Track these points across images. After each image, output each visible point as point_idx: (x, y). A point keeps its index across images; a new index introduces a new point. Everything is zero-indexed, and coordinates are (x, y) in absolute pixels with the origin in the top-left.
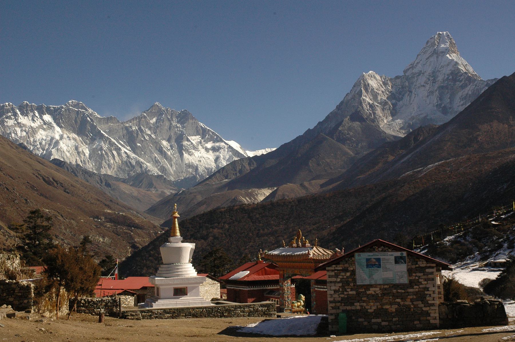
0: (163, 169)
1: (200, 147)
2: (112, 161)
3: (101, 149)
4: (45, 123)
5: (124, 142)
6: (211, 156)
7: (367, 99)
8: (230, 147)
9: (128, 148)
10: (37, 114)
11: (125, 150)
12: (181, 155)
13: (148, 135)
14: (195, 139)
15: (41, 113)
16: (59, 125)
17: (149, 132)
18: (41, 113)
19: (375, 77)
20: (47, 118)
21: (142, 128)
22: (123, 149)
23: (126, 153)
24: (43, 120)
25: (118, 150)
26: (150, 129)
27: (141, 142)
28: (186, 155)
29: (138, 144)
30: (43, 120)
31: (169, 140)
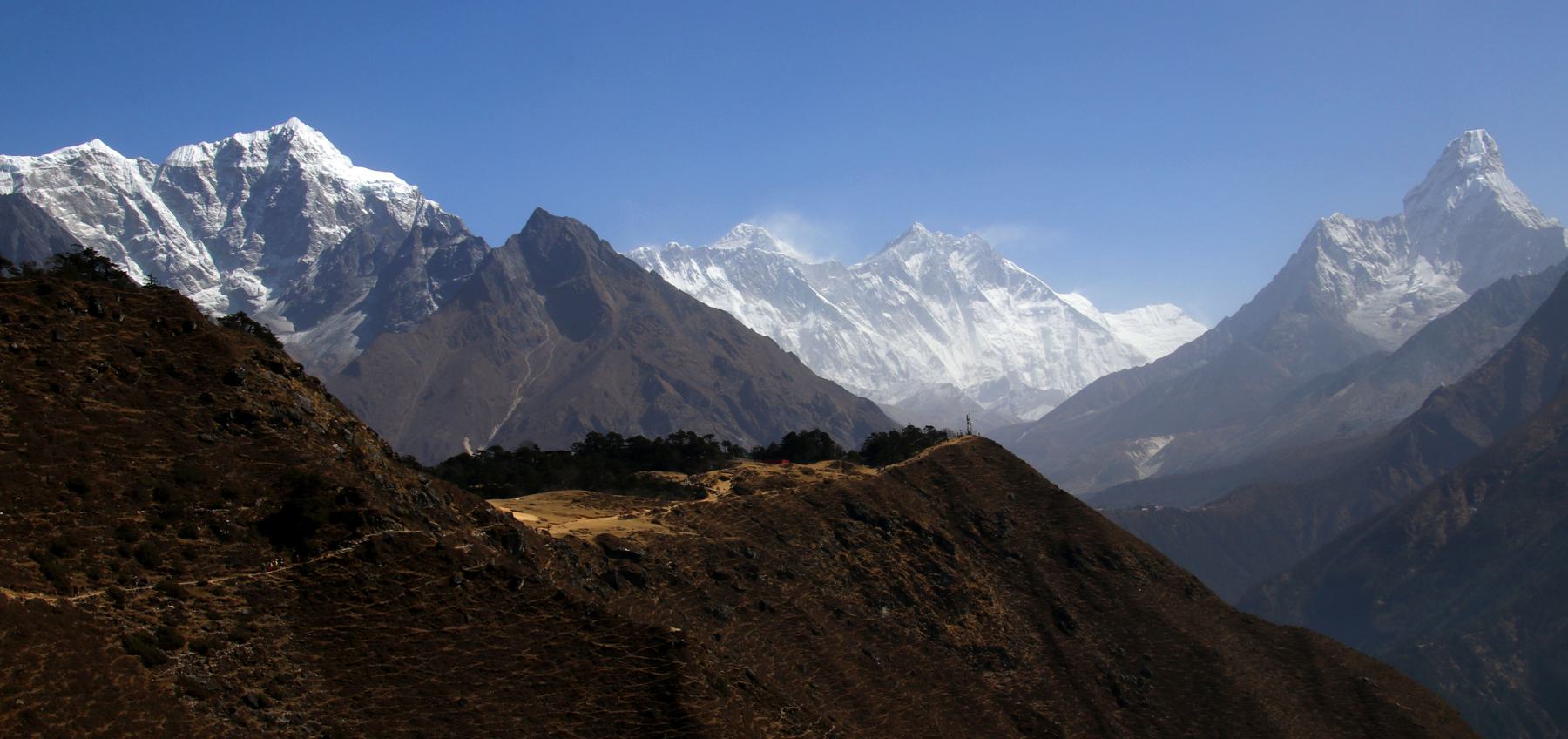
0: (935, 362)
1: (1007, 314)
2: (842, 353)
3: (821, 330)
4: (712, 284)
5: (859, 312)
6: (1030, 328)
7: (1328, 265)
8: (1071, 310)
9: (867, 322)
10: (696, 267)
11: (864, 327)
12: (971, 329)
13: (902, 293)
14: (996, 296)
15: (704, 264)
16: (738, 287)
17: (905, 288)
18: (704, 264)
19: (1343, 224)
20: (715, 272)
21: (892, 279)
22: (862, 329)
23: (866, 335)
24: (707, 277)
25: (849, 326)
26: (908, 280)
27: (891, 309)
28: (980, 330)
29: (887, 315)
30: (707, 277)
31: (945, 302)
